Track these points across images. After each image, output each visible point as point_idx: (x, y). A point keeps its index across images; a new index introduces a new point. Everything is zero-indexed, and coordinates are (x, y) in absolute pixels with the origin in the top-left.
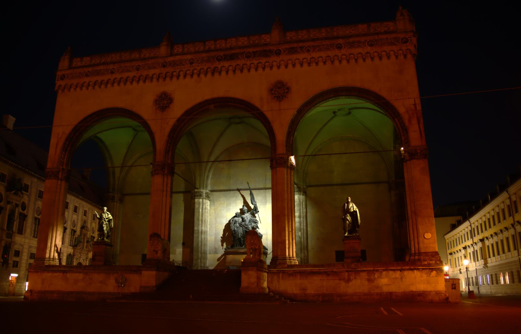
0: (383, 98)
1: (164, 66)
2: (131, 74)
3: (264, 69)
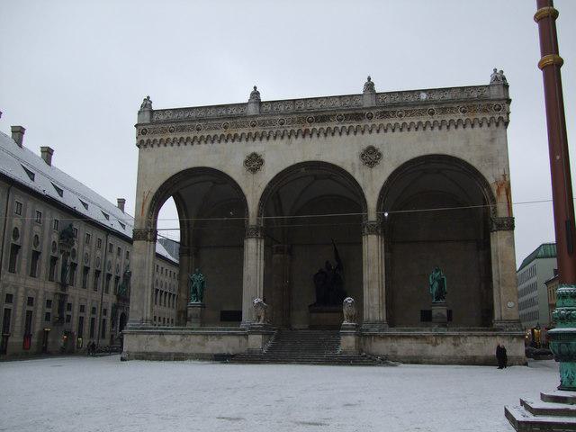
0: (473, 167)
2: (219, 133)
3: (355, 133)
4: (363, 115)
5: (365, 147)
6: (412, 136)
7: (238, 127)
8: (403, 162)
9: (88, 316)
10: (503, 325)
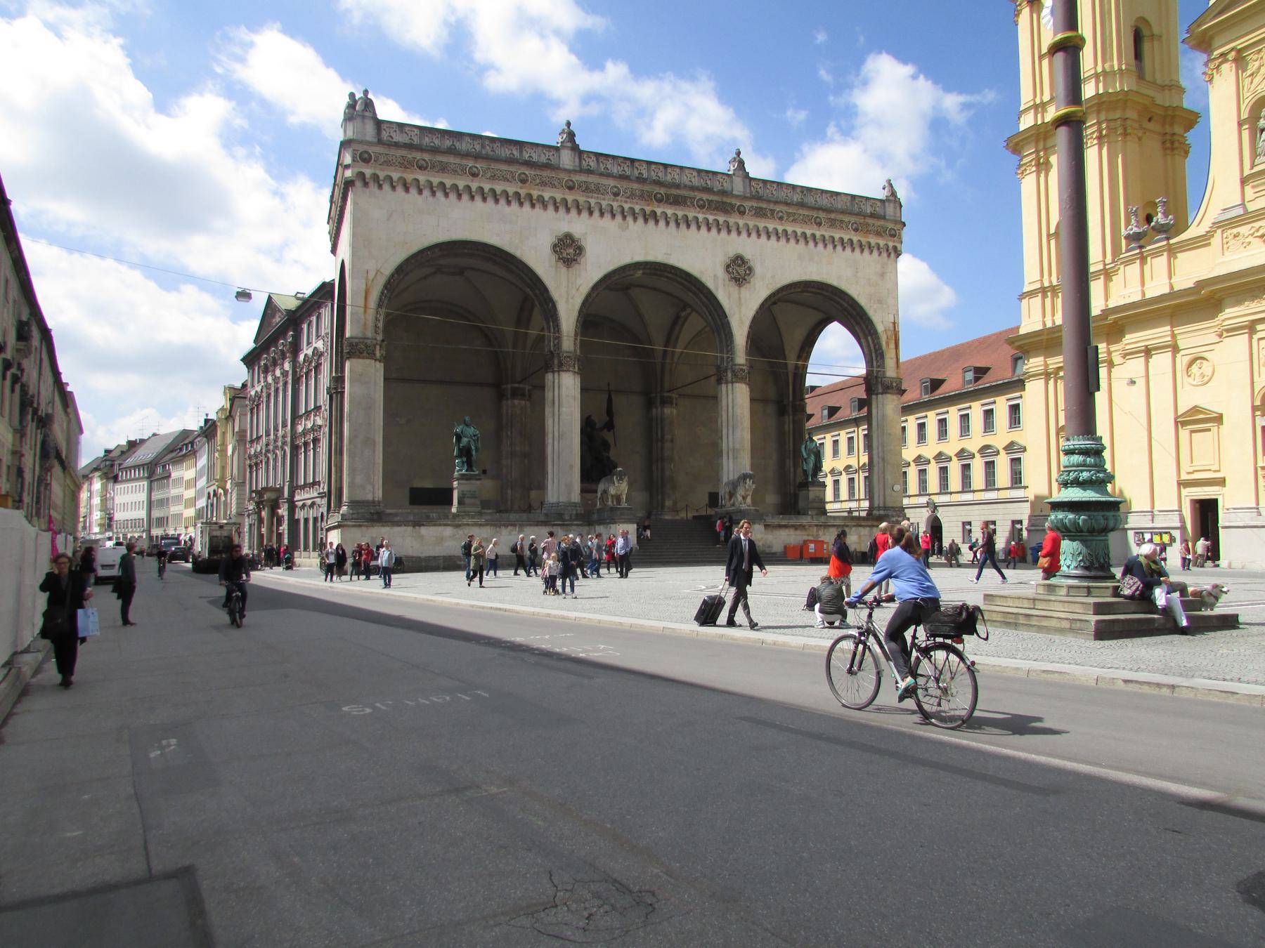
1: (571, 188)
4: (732, 206)
5: (732, 254)
6: (791, 251)
7: (543, 184)
8: (779, 286)
10: (890, 513)
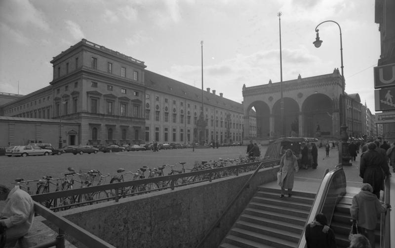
9: (235, 135)
